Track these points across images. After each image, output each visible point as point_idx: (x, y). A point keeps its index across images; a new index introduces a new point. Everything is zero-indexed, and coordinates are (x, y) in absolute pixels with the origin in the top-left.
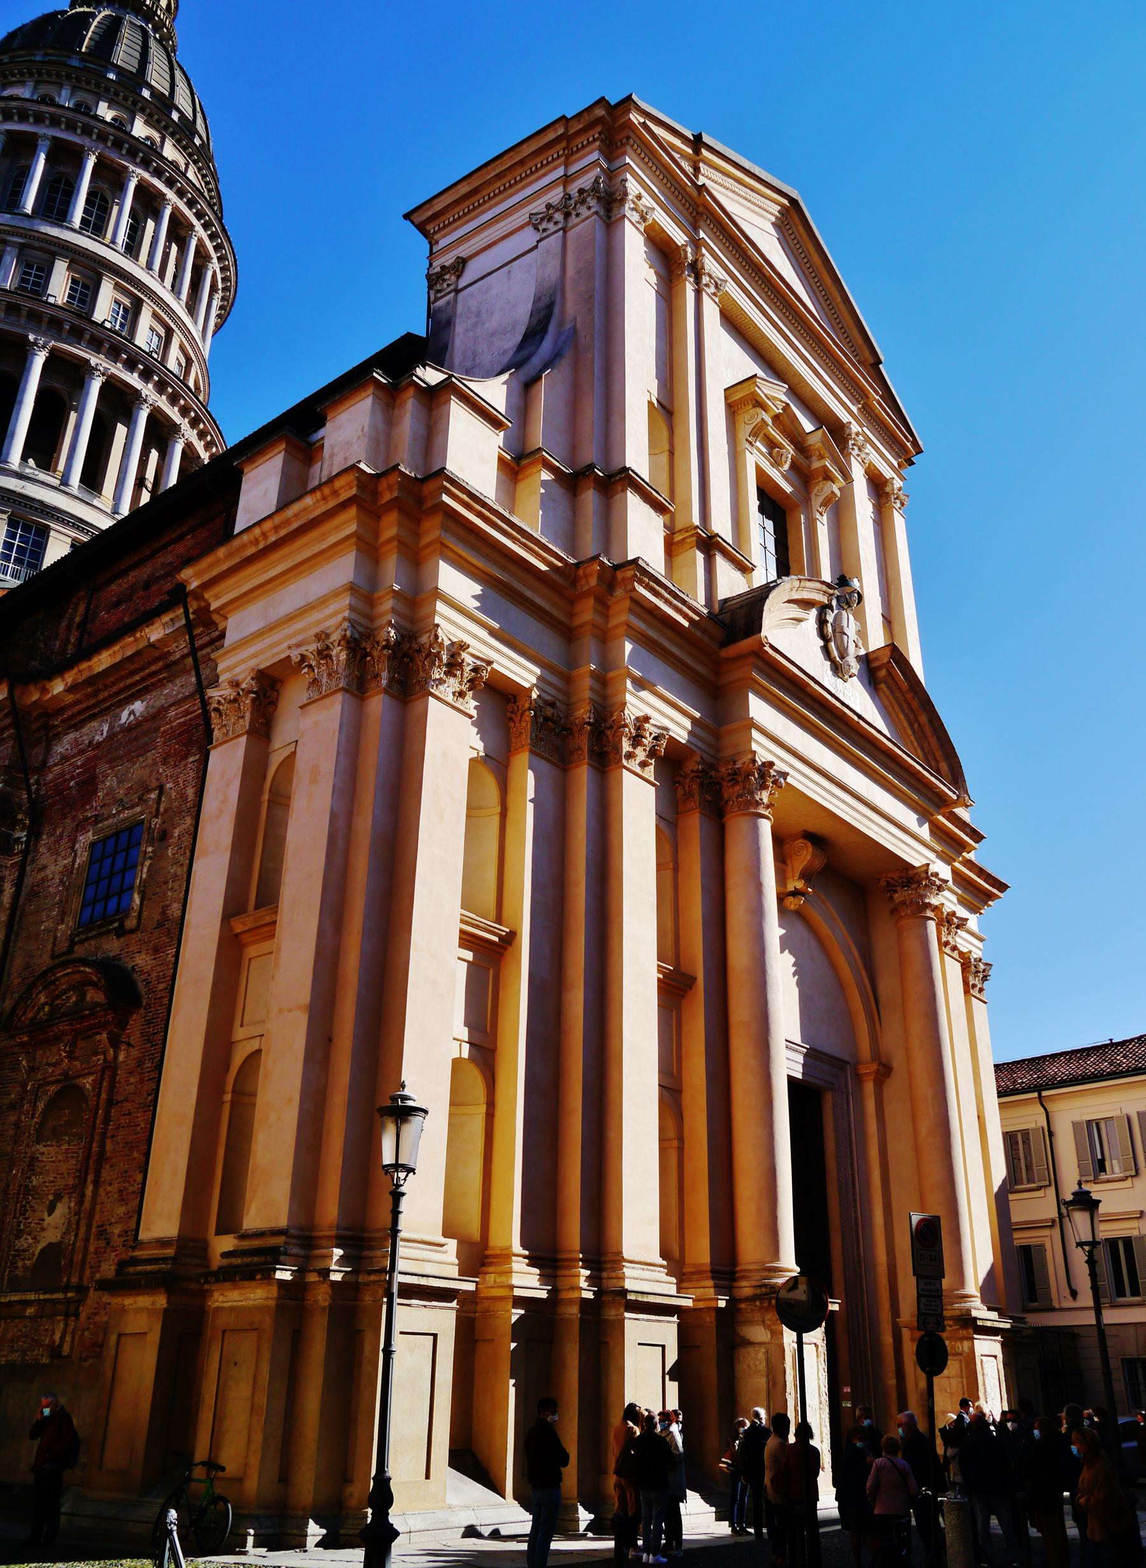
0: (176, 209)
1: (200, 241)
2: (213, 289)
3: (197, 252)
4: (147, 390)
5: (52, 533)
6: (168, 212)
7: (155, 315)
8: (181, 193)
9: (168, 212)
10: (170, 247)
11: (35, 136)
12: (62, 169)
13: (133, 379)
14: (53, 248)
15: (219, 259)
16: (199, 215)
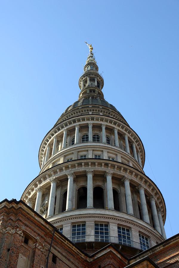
0: (118, 130)
1: (129, 137)
2: (137, 151)
3: (129, 142)
4: (127, 175)
5: (110, 224)
6: (116, 132)
7: (122, 157)
8: (119, 126)
9: (116, 132)
10: (121, 142)
11: (75, 126)
12: (84, 133)
13: (122, 173)
14: (87, 149)
15: (136, 142)
16: (126, 130)
